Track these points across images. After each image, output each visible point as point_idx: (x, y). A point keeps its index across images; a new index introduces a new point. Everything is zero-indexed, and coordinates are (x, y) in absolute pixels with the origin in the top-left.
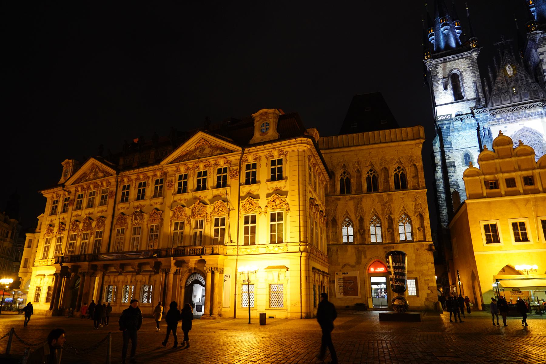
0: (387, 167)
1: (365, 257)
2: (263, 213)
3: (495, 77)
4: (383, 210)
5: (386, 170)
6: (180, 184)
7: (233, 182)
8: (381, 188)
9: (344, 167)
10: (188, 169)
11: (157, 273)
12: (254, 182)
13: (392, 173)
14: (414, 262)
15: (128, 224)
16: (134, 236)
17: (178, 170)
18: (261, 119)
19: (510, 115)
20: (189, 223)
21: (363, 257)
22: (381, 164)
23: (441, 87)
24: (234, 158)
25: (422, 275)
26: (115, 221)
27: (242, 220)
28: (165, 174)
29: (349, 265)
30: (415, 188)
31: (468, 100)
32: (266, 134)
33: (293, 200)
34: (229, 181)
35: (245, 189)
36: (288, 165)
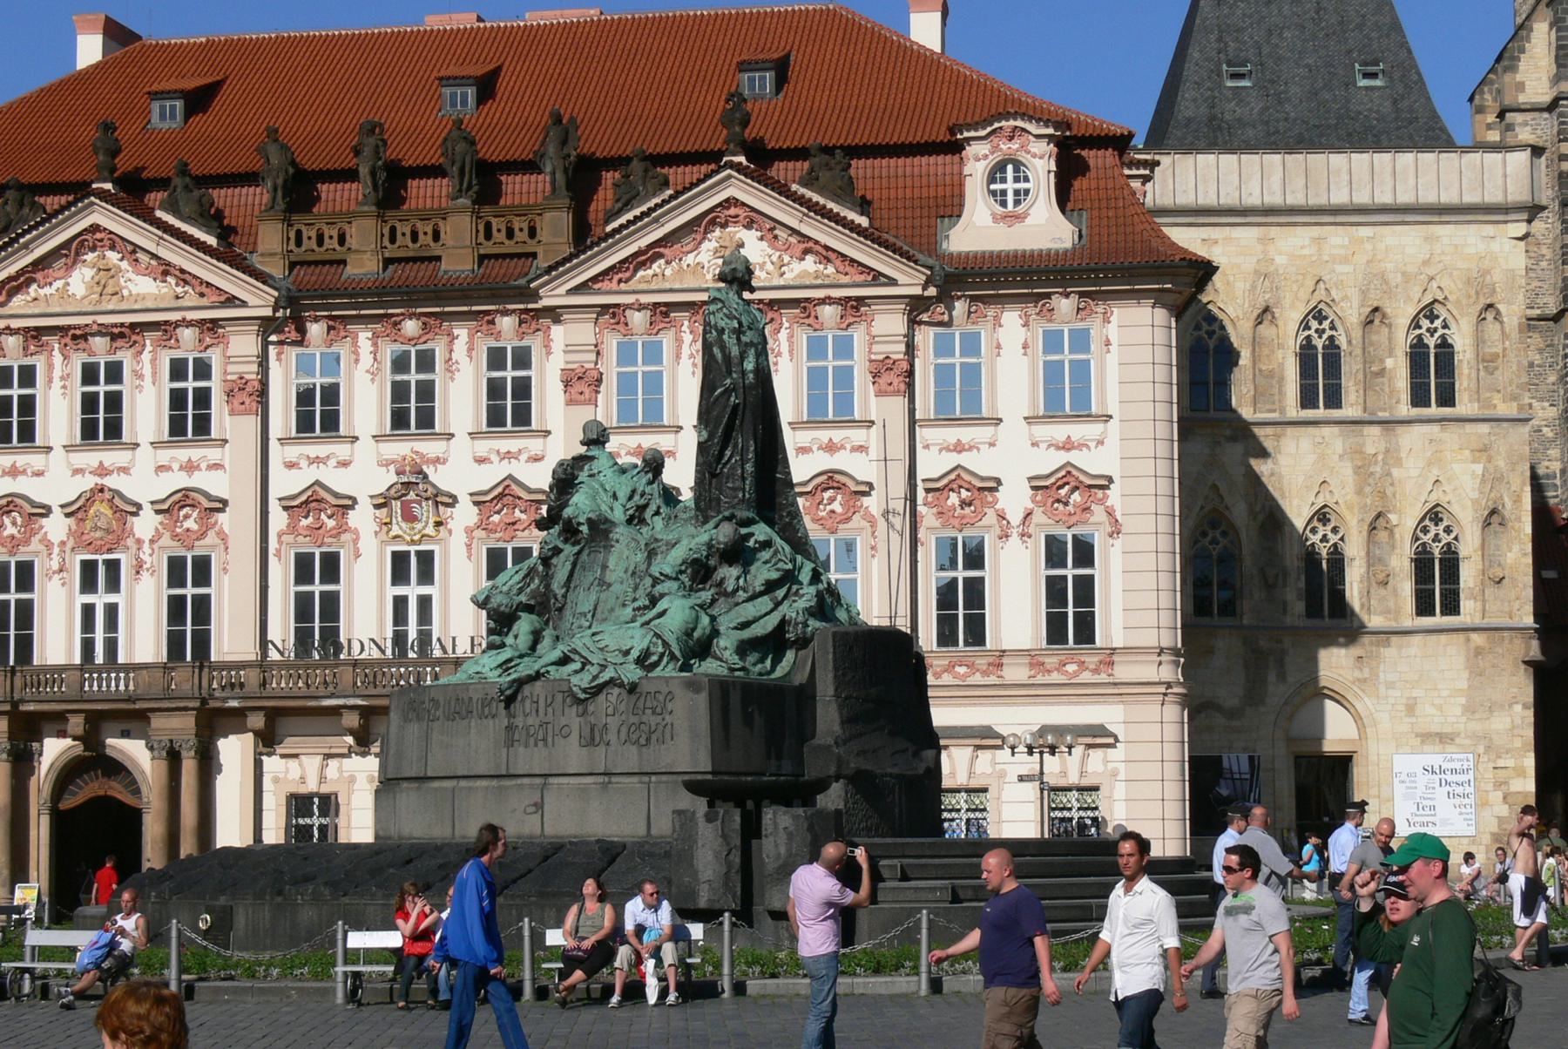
0: (1388, 311)
1: (1282, 677)
2: (1015, 533)
4: (1359, 492)
6: (626, 384)
13: (1402, 340)
14: (1463, 701)
15: (356, 532)
16: (400, 591)
18: (995, 149)
21: (1272, 677)
22: (1364, 293)
25: (1488, 748)
26: (278, 519)
29: (1218, 708)
32: (1020, 218)
36: (1112, 359)
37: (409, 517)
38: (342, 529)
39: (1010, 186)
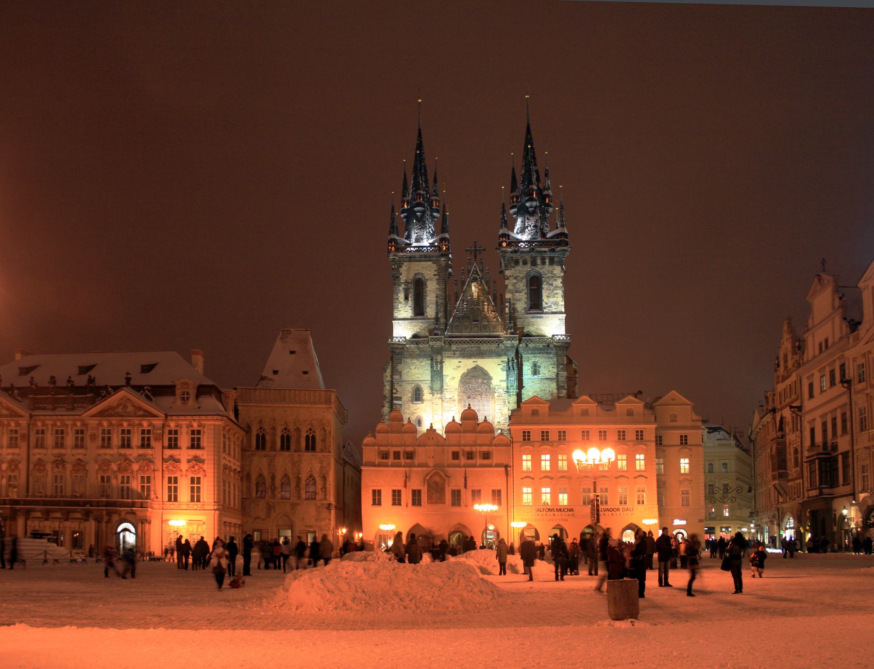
5: (298, 430)
6: (103, 439)
7: (157, 445)
8: (292, 447)
9: (260, 422)
10: (110, 424)
11: (87, 520)
12: (176, 447)
13: (304, 435)
17: (100, 424)
20: (116, 477)
23: (401, 296)
24: (158, 423)
26: (31, 466)
27: (166, 480)
28: (85, 425)
30: (322, 451)
33: (209, 467)
34: (153, 443)
35: (168, 453)
36: (205, 436)
38: (45, 469)
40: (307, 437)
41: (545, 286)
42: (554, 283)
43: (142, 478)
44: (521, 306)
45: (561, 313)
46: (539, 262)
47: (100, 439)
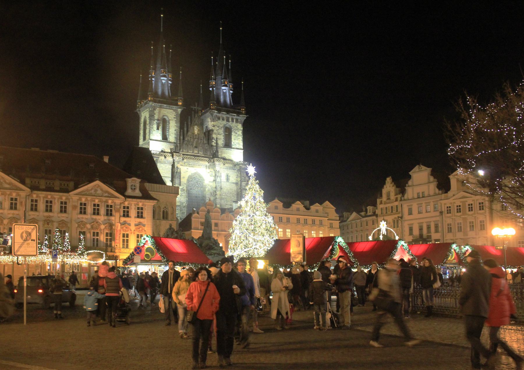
3: (188, 131)
7: (117, 215)
10: (86, 200)
13: (162, 210)
19: (191, 162)
20: (90, 232)
23: (155, 126)
24: (118, 201)
31: (170, 142)
34: (113, 213)
35: (123, 219)
36: (146, 211)
37: (48, 224)
39: (133, 187)
40: (164, 211)
41: (233, 133)
42: (238, 133)
43: (94, 233)
44: (221, 142)
45: (241, 149)
46: (230, 120)
47: (79, 208)
